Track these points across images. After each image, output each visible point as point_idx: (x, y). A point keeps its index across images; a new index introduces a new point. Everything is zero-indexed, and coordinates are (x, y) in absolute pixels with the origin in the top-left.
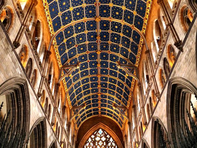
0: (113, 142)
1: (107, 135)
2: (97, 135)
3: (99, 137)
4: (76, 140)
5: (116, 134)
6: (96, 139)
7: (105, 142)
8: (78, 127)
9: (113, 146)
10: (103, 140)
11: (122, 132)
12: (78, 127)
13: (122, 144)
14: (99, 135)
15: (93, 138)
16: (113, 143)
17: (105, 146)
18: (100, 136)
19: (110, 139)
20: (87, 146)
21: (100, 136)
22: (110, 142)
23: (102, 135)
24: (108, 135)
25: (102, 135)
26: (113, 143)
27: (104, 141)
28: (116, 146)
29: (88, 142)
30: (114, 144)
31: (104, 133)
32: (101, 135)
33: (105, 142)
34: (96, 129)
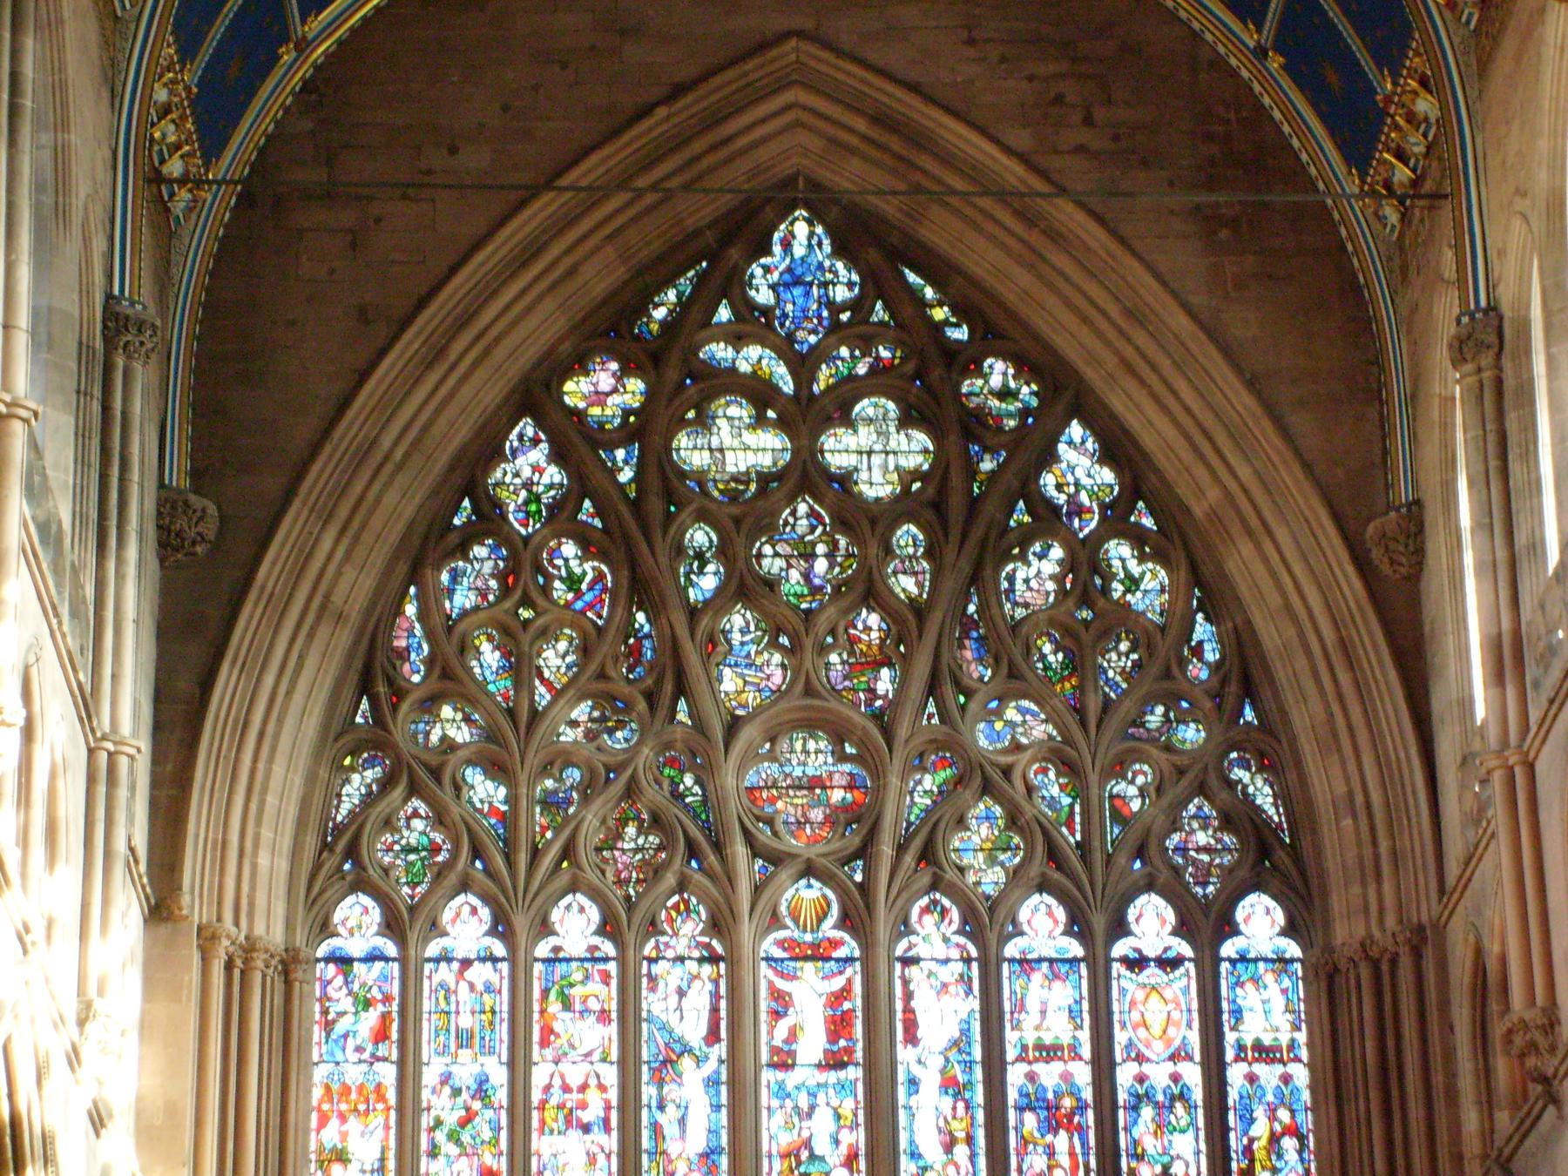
0: (1116, 519)
1: (968, 361)
2: (720, 352)
3: (759, 392)
4: (178, 477)
5: (1213, 333)
6: (690, 452)
7: (908, 536)
8: (212, 141)
9: (1120, 620)
10: (876, 485)
11: (1352, 292)
12: (212, 141)
13: (1352, 585)
14: (752, 357)
15: (610, 411)
16: (1119, 552)
17: (919, 609)
18: (788, 387)
19: (1048, 457)
20: (463, 599)
21: (788, 387)
22: (1049, 519)
23: (848, 361)
24: (998, 371)
25: (848, 361)
26: (1119, 552)
27: (902, 507)
28: (1202, 630)
29: (490, 519)
30: (1154, 577)
31: (880, 313)
32: (803, 366)
33: (908, 536)
34: (699, 211)
